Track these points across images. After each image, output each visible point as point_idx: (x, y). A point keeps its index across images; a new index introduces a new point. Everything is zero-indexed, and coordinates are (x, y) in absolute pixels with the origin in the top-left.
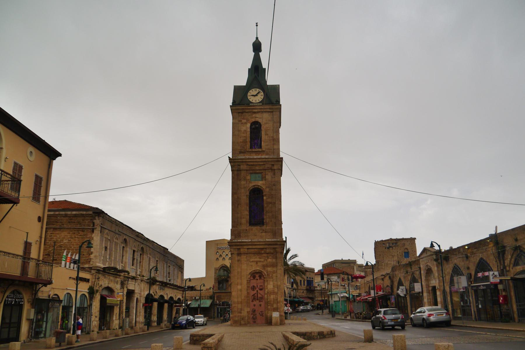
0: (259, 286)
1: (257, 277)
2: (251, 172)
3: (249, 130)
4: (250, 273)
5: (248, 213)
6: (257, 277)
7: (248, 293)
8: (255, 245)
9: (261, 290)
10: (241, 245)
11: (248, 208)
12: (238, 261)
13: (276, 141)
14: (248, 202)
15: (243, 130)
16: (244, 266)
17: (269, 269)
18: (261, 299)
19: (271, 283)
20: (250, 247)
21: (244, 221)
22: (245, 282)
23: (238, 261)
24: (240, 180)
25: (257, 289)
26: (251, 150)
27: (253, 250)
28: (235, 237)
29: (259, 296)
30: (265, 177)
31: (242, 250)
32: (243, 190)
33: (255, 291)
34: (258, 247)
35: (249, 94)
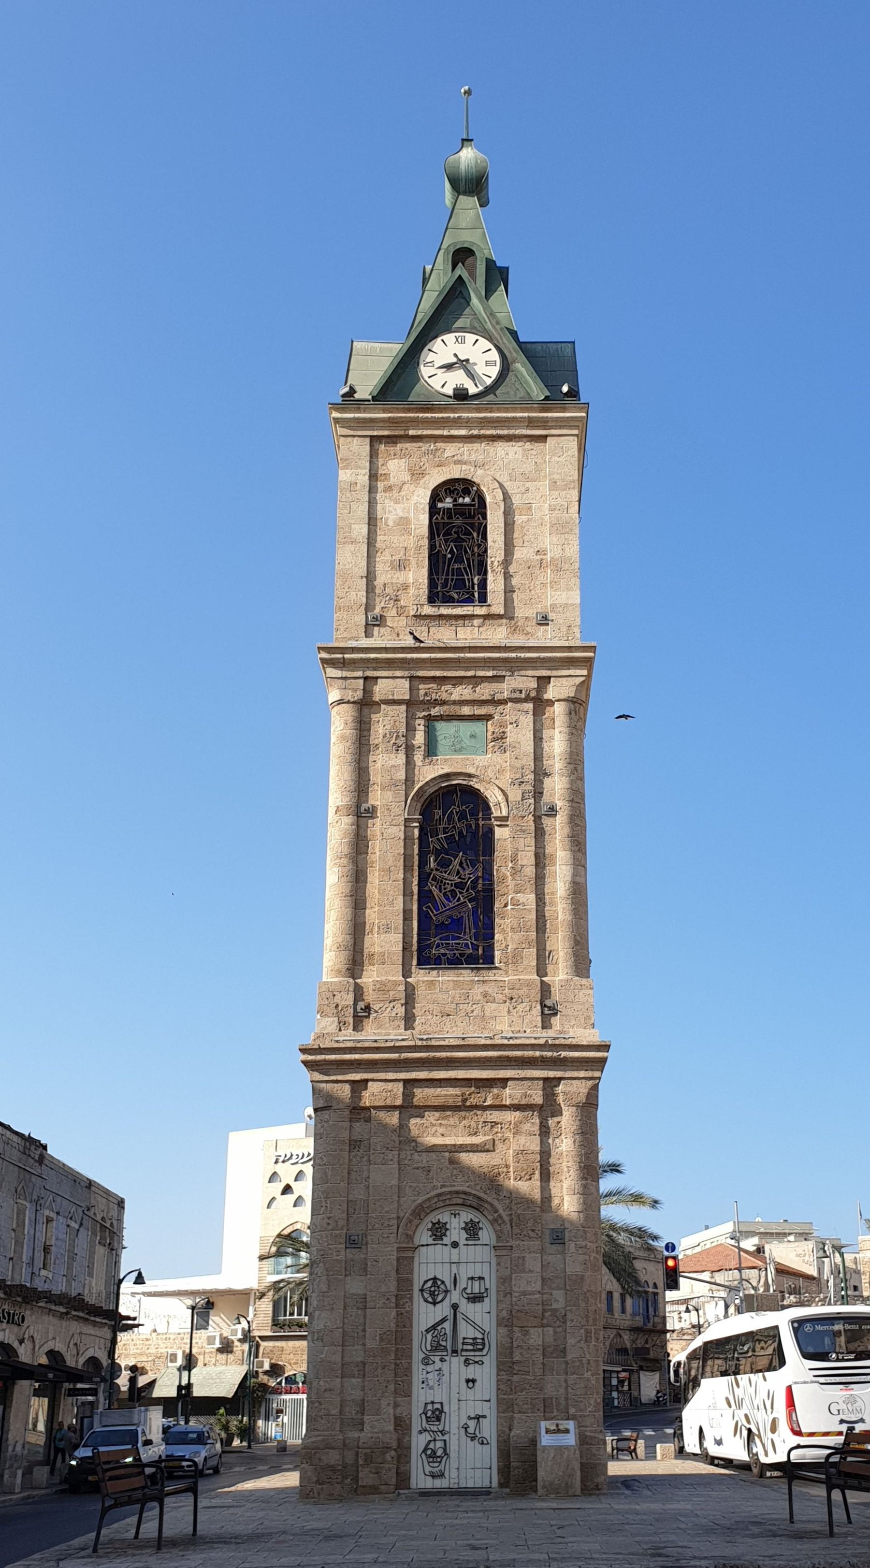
0: (462, 1284)
1: (456, 1232)
3: (425, 519)
9: (475, 1299)
12: (354, 1144)
15: (391, 519)
25: (455, 1296)
26: (428, 610)
28: (342, 1025)
29: (466, 1331)
30: (502, 737)
33: (443, 1310)
35: (427, 356)
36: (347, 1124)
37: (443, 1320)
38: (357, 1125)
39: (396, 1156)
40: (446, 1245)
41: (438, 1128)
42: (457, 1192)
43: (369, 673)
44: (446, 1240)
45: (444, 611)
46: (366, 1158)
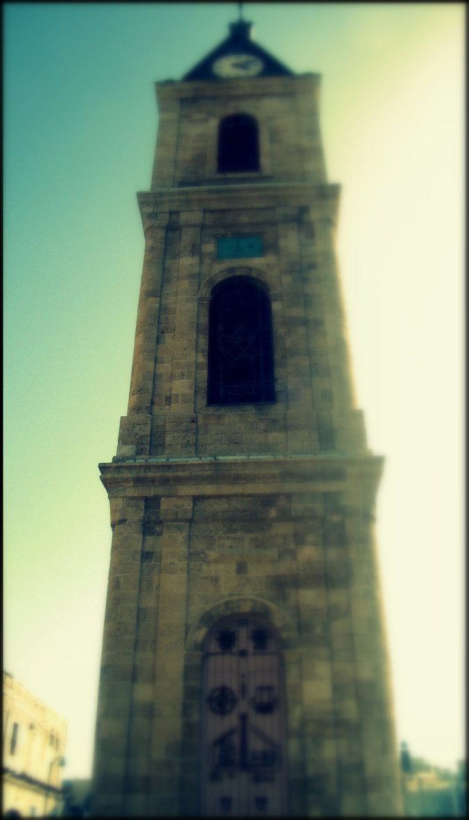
0: (251, 692)
1: (244, 640)
2: (221, 231)
4: (206, 619)
5: (202, 359)
6: (244, 640)
7: (190, 729)
8: (236, 479)
9: (265, 708)
10: (165, 481)
11: (204, 342)
13: (311, 150)
14: (205, 320)
16: (173, 583)
17: (309, 597)
18: (265, 763)
19: (323, 669)
20: (209, 489)
21: (181, 387)
22: (172, 662)
23: (146, 556)
24: (176, 256)
25: (243, 706)
27: (222, 506)
28: (139, 452)
31: (165, 504)
32: (185, 285)
33: (231, 721)
34: (250, 489)
36: (141, 536)
37: (231, 732)
38: (149, 539)
39: (186, 566)
40: (235, 654)
41: (226, 541)
42: (245, 600)
43: (174, 208)
44: (235, 650)
45: (229, 176)
46: (156, 569)
